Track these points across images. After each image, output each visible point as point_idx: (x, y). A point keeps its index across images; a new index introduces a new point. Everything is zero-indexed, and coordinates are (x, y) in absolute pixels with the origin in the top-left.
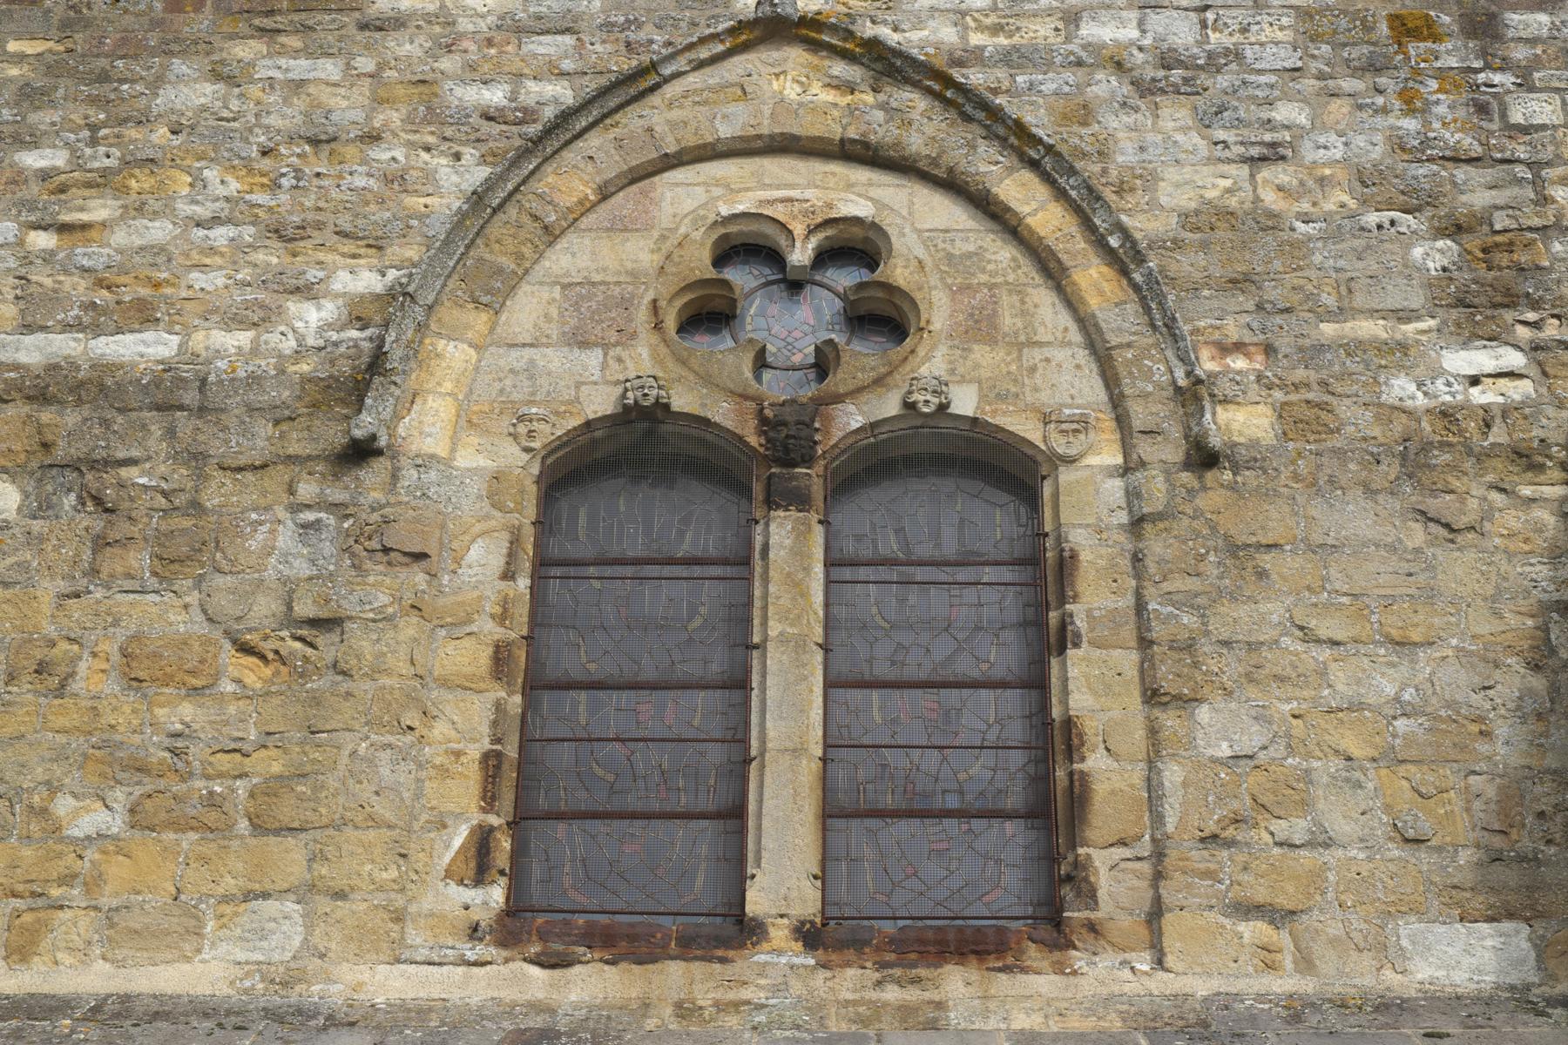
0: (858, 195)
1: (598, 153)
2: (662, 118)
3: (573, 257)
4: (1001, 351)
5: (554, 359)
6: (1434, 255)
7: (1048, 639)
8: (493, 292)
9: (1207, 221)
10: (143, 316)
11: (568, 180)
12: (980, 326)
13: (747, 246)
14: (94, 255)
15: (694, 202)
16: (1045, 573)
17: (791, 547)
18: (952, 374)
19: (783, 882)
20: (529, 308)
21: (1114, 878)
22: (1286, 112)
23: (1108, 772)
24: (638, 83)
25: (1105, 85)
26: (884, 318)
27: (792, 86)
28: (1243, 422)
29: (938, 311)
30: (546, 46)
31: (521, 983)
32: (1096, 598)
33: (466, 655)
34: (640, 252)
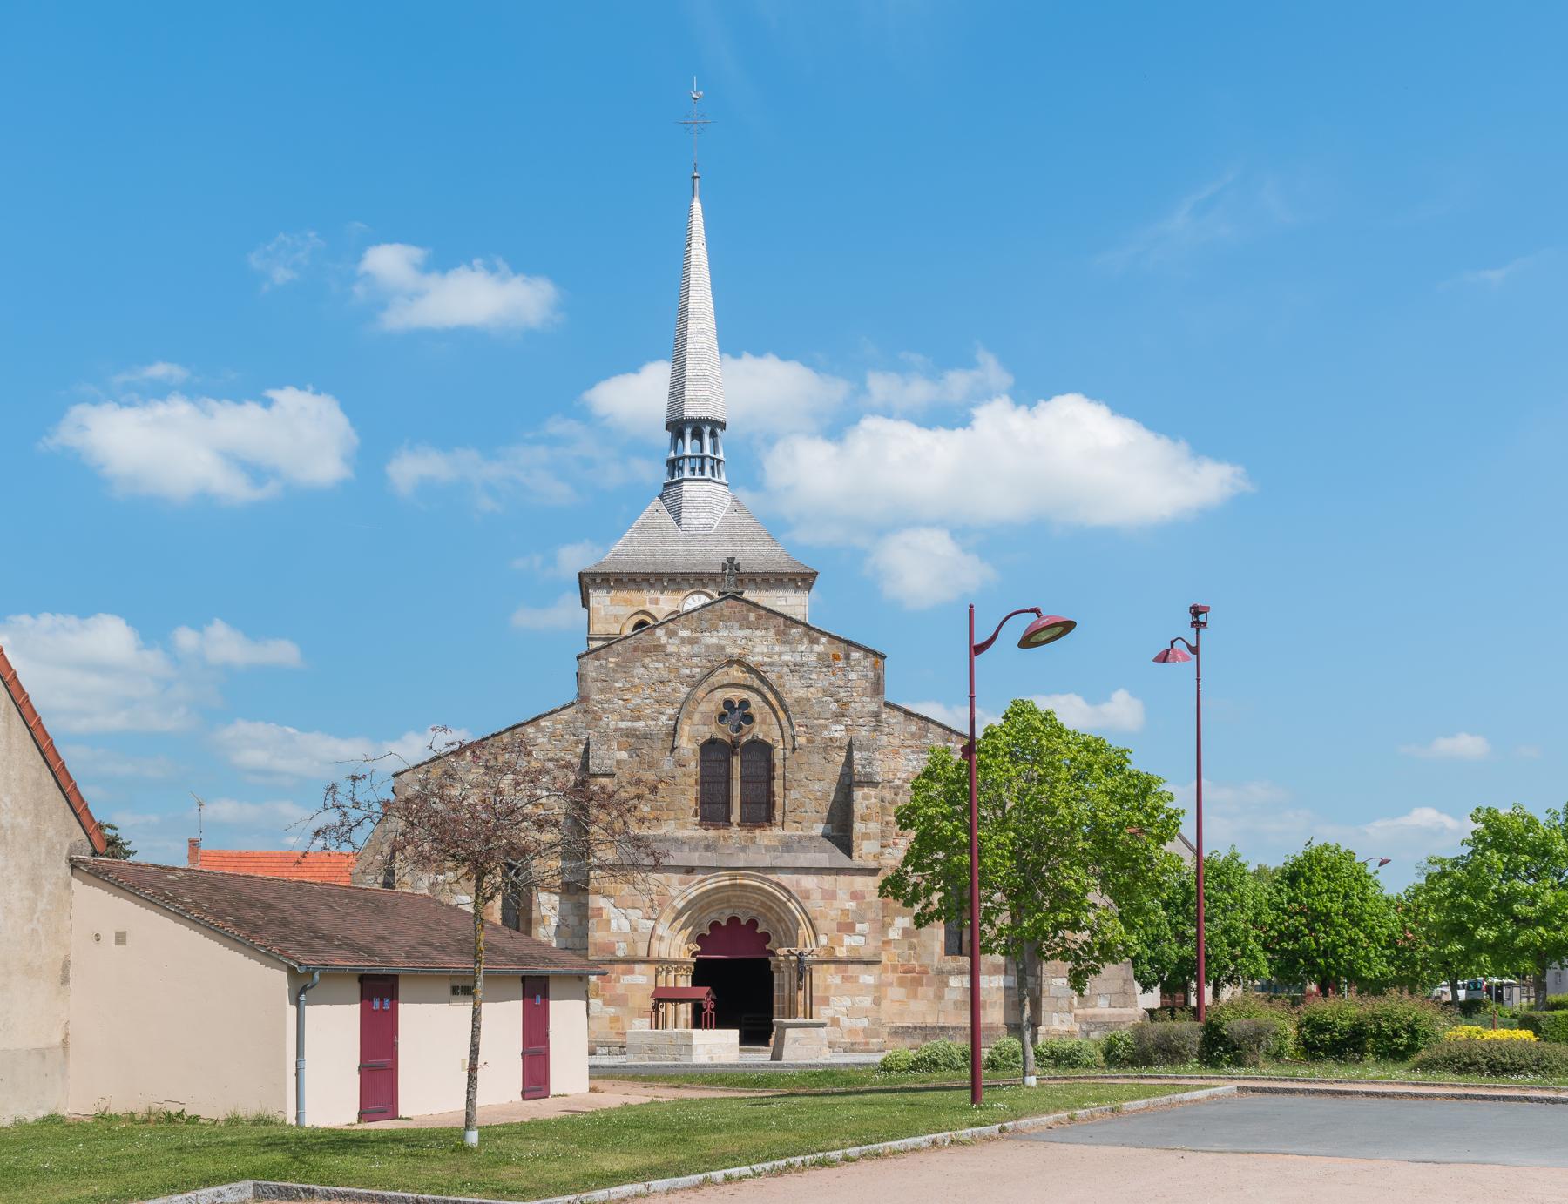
0: (746, 695)
1: (705, 687)
2: (715, 679)
3: (703, 707)
4: (765, 728)
5: (701, 728)
6: (834, 706)
7: (771, 778)
8: (690, 716)
9: (798, 700)
10: (639, 718)
11: (700, 693)
12: (764, 722)
13: (728, 704)
14: (630, 705)
15: (721, 695)
16: (771, 767)
17: (736, 762)
18: (758, 731)
19: (735, 816)
20: (697, 718)
21: (778, 816)
22: (814, 676)
23: (778, 800)
24: (711, 673)
25: (786, 670)
26: (749, 719)
27: (736, 673)
28: (801, 740)
29: (757, 719)
30: (696, 660)
31: (701, 832)
32: (778, 772)
33: (692, 781)
34: (712, 706)
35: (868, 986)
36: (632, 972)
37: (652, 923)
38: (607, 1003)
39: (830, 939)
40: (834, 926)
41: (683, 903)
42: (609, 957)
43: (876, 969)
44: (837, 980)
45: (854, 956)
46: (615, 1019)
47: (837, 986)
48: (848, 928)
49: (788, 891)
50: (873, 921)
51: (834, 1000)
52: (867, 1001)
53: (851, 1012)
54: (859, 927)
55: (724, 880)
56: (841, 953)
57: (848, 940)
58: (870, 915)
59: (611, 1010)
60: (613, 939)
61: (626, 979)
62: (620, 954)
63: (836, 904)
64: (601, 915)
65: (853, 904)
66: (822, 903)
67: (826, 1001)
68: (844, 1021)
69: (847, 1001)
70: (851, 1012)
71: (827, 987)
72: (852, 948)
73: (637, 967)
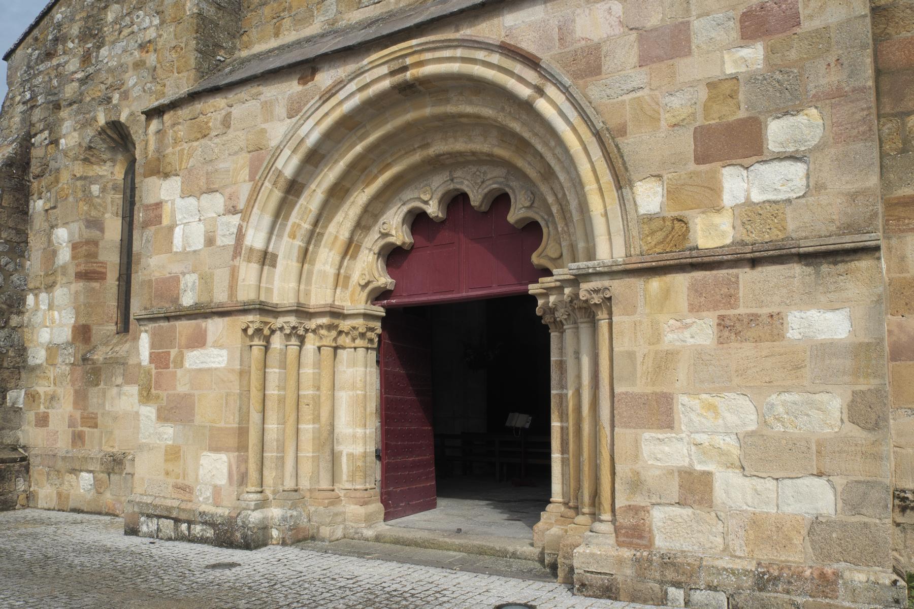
35: (825, 350)
36: (198, 341)
37: (235, 220)
38: (164, 416)
39: (672, 194)
40: (686, 143)
41: (295, 161)
42: (169, 307)
43: (858, 281)
44: (701, 332)
45: (761, 235)
46: (173, 454)
47: (700, 356)
48: (734, 140)
49: (532, 62)
50: (834, 97)
51: (688, 407)
52: (826, 411)
53: (764, 453)
54: (777, 132)
55: (375, 75)
56: (712, 232)
57: (737, 185)
58: (824, 77)
59: (169, 431)
60: (176, 268)
61: (194, 359)
62: (187, 300)
63: (694, 69)
64: (158, 219)
65: (753, 56)
66: (639, 77)
67: (660, 412)
68: (734, 489)
69: (739, 412)
70: (764, 453)
71: (665, 362)
72: (750, 212)
73: (215, 327)
